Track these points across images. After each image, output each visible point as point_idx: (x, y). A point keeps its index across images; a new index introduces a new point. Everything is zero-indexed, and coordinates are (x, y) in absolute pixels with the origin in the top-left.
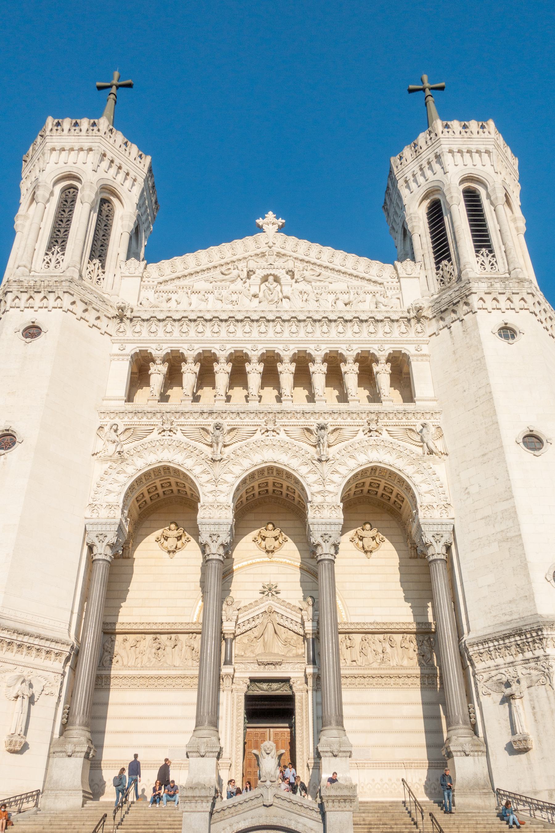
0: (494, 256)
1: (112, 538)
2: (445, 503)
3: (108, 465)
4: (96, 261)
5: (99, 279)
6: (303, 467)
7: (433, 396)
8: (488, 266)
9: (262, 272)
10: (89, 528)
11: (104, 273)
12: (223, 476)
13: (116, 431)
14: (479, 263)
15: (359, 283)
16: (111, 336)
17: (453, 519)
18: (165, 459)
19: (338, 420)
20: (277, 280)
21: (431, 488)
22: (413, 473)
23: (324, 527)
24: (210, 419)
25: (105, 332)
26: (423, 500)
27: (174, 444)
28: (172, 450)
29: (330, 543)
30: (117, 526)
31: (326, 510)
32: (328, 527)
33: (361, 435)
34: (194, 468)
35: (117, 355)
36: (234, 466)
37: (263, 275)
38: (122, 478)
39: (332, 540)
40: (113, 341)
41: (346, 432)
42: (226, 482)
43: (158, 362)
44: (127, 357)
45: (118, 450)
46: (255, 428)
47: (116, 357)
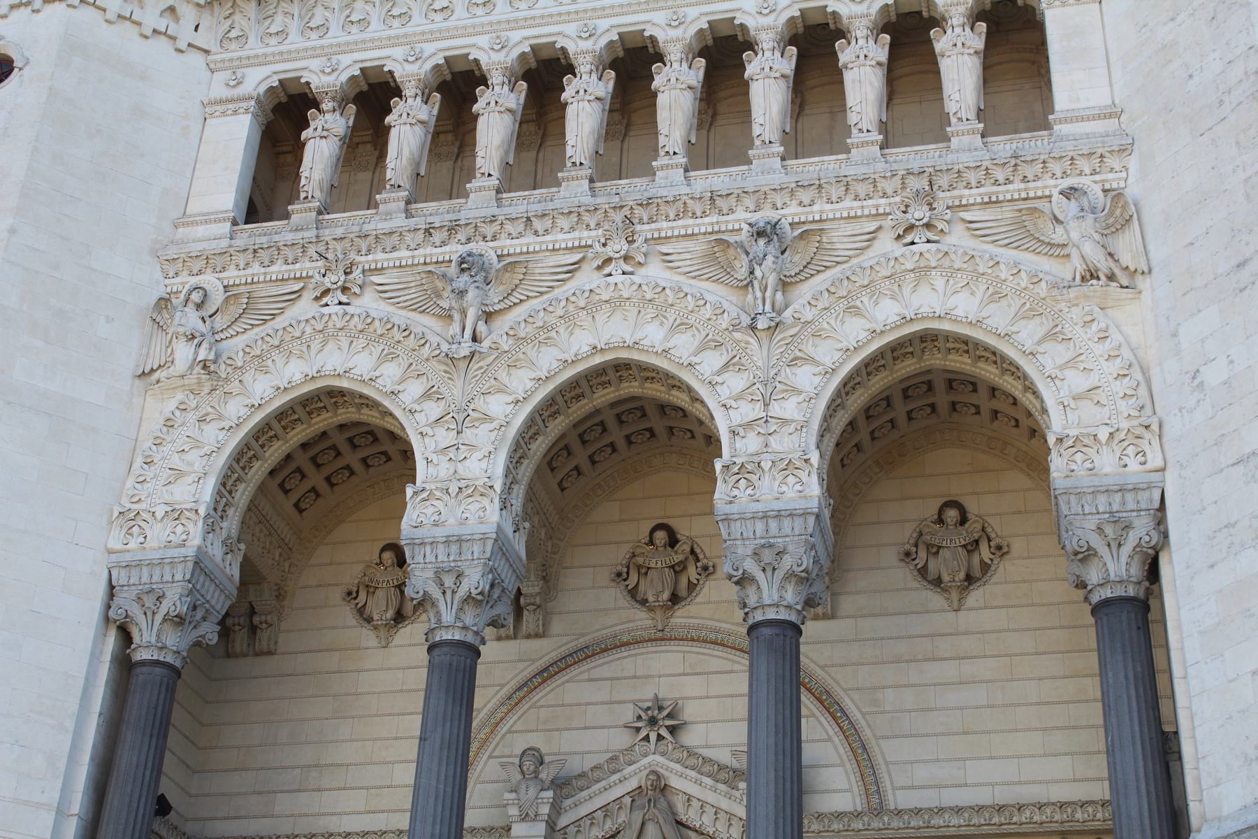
1: (174, 601)
2: (1136, 422)
3: (172, 404)
6: (708, 353)
7: (1110, 102)
10: (120, 577)
12: (479, 403)
13: (199, 306)
16: (207, 52)
17: (1163, 470)
19: (816, 208)
21: (1093, 380)
22: (1039, 343)
23: (760, 527)
25: (189, 45)
27: (352, 323)
28: (344, 343)
29: (779, 574)
30: (190, 565)
31: (767, 479)
32: (773, 525)
33: (886, 244)
34: (400, 388)
35: (221, 102)
36: (513, 371)
38: (211, 433)
39: (787, 562)
40: (212, 66)
41: (840, 237)
42: (487, 418)
43: (327, 105)
44: (245, 105)
45: (200, 358)
47: (219, 108)
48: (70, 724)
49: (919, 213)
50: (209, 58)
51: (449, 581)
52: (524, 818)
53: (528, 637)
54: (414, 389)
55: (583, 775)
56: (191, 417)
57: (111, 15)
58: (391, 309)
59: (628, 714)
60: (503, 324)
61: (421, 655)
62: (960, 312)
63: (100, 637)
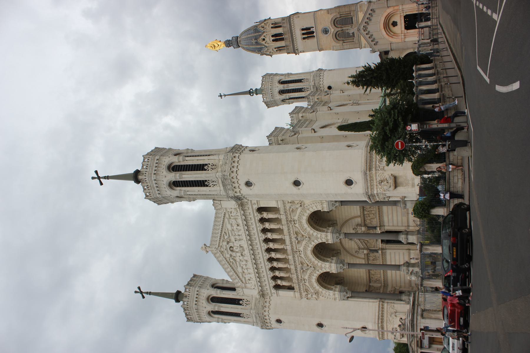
0: (209, 180)
4: (241, 302)
5: (247, 301)
8: (214, 183)
9: (230, 252)
11: (244, 299)
13: (307, 295)
14: (214, 186)
15: (226, 220)
17: (326, 201)
18: (315, 281)
19: (292, 232)
20: (231, 247)
24: (298, 270)
25: (270, 299)
26: (319, 208)
37: (231, 252)
41: (297, 230)
43: (277, 283)
44: (277, 292)
46: (299, 257)
47: (278, 295)
48: (360, 302)
49: (293, 223)
50: (270, 296)
51: (342, 268)
52: (363, 252)
53: (340, 251)
54: (317, 272)
55: (358, 246)
56: (322, 294)
57: (269, 309)
58: (307, 275)
59: (350, 241)
60: (309, 264)
61: (350, 269)
62: (306, 218)
63: (349, 300)
